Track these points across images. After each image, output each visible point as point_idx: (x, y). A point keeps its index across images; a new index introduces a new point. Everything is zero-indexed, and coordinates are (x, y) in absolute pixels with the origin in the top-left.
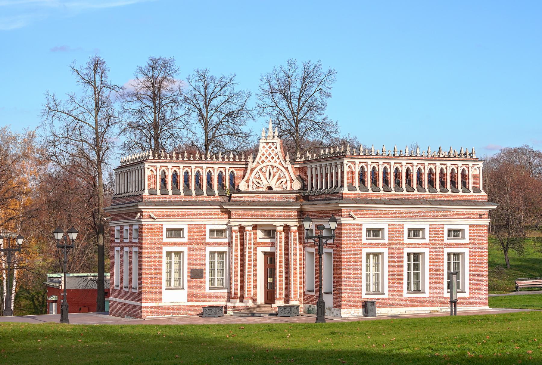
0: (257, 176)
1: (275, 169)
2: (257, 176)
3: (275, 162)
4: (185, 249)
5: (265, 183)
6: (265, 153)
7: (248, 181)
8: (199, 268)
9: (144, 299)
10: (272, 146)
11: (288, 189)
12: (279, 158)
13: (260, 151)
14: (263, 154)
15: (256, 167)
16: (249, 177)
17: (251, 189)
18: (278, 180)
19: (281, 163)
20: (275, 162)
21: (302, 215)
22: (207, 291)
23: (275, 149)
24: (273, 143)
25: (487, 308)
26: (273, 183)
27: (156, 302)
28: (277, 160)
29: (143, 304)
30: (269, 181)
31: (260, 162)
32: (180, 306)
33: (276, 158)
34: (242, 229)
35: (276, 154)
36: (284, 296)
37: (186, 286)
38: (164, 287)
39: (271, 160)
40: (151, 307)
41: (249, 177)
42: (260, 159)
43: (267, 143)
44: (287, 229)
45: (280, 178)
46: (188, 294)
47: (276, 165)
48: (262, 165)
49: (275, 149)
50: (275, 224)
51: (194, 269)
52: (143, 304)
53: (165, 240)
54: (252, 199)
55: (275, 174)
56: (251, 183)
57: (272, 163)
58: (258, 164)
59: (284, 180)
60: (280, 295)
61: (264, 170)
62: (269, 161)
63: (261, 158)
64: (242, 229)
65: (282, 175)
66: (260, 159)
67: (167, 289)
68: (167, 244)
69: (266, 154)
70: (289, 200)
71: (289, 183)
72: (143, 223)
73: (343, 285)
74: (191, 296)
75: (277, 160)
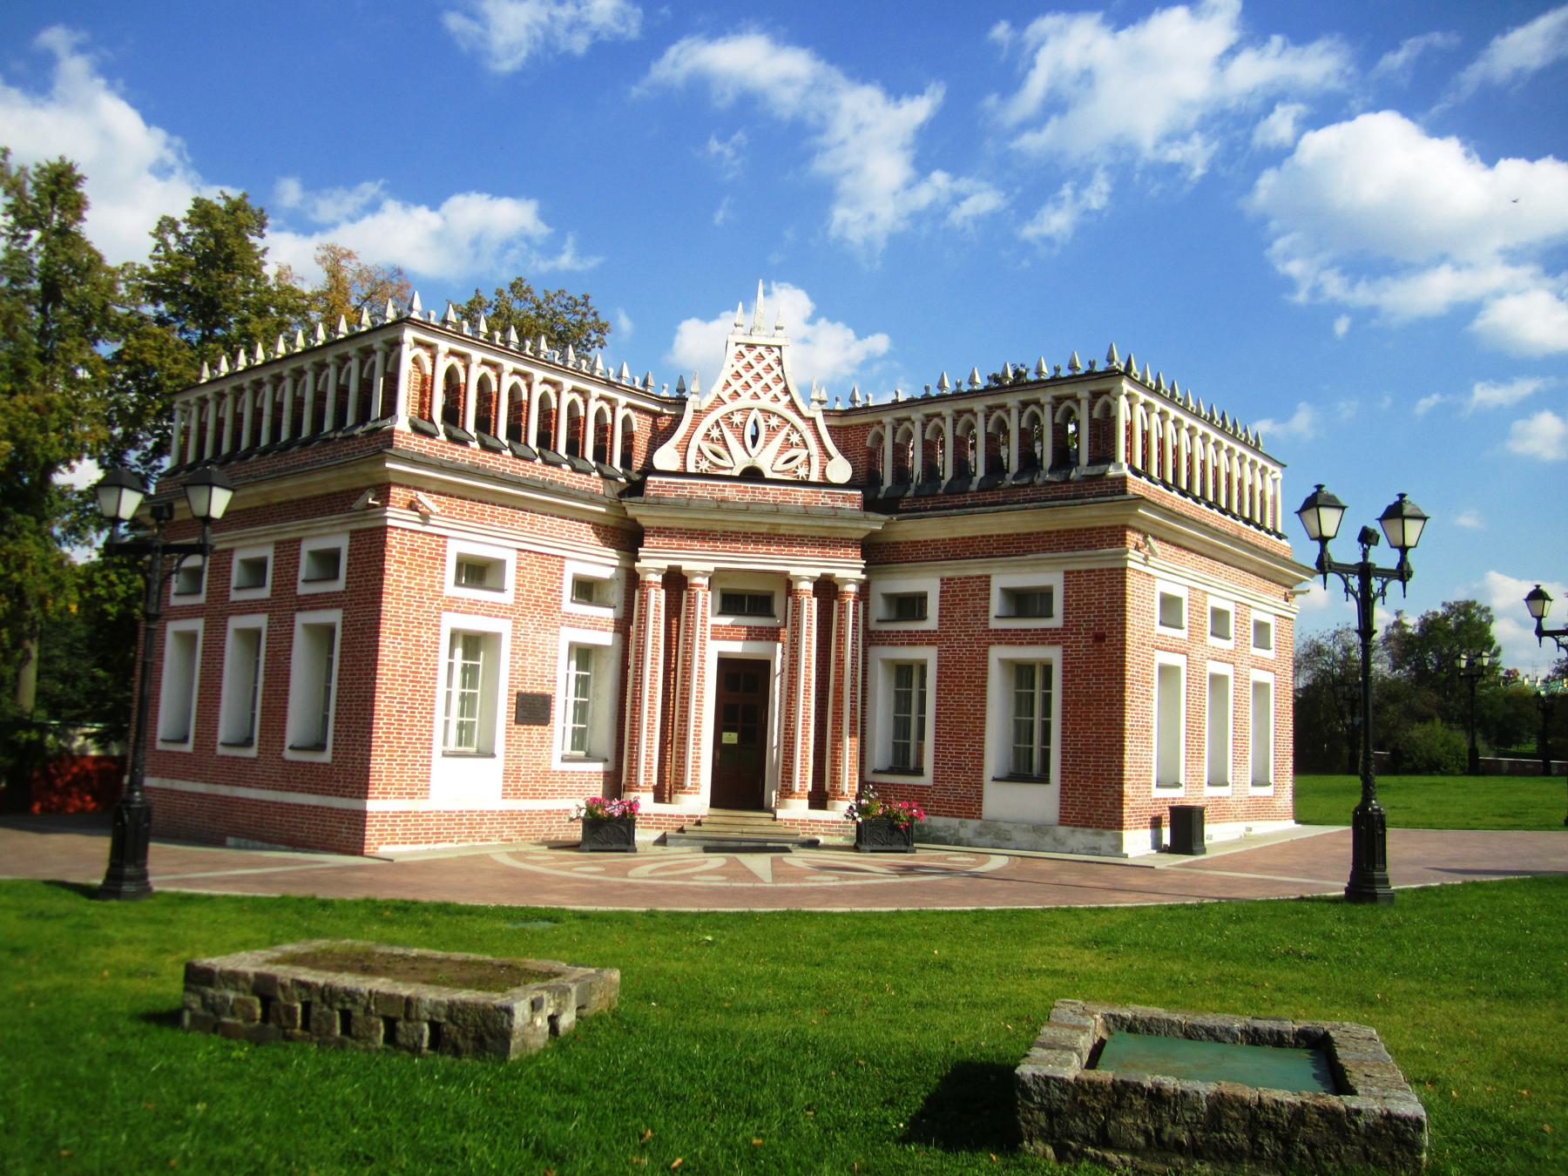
0: (715, 433)
1: (774, 421)
2: (715, 433)
3: (776, 399)
4: (501, 626)
5: (739, 461)
6: (742, 372)
7: (684, 448)
8: (538, 690)
9: (376, 784)
10: (765, 354)
11: (814, 477)
12: (786, 391)
13: (727, 365)
14: (738, 375)
15: (712, 408)
16: (688, 438)
17: (691, 469)
18: (780, 452)
19: (792, 405)
20: (776, 399)
21: (876, 553)
22: (557, 765)
23: (774, 365)
24: (768, 347)
25: (1290, 824)
26: (767, 459)
27: (412, 795)
28: (781, 395)
29: (372, 806)
30: (753, 452)
31: (725, 396)
32: (482, 814)
33: (777, 389)
34: (676, 582)
35: (778, 379)
36: (810, 788)
37: (500, 747)
38: (438, 747)
39: (760, 393)
40: (396, 815)
41: (688, 438)
42: (725, 388)
43: (751, 346)
44: (827, 589)
45: (788, 444)
46: (506, 773)
47: (781, 407)
48: (731, 406)
49: (774, 365)
50: (794, 571)
51: (526, 695)
52: (372, 806)
53: (451, 589)
54: (718, 495)
55: (773, 431)
56: (692, 454)
57: (765, 401)
58: (720, 401)
59: (803, 454)
60: (803, 783)
61: (737, 419)
62: (756, 396)
63: (729, 384)
64: (676, 582)
65: (795, 438)
66: (725, 388)
67: (445, 755)
68: (452, 605)
69: (747, 376)
70: (840, 504)
71: (815, 461)
72: (390, 522)
73: (1127, 758)
74: (514, 784)
75: (781, 395)
